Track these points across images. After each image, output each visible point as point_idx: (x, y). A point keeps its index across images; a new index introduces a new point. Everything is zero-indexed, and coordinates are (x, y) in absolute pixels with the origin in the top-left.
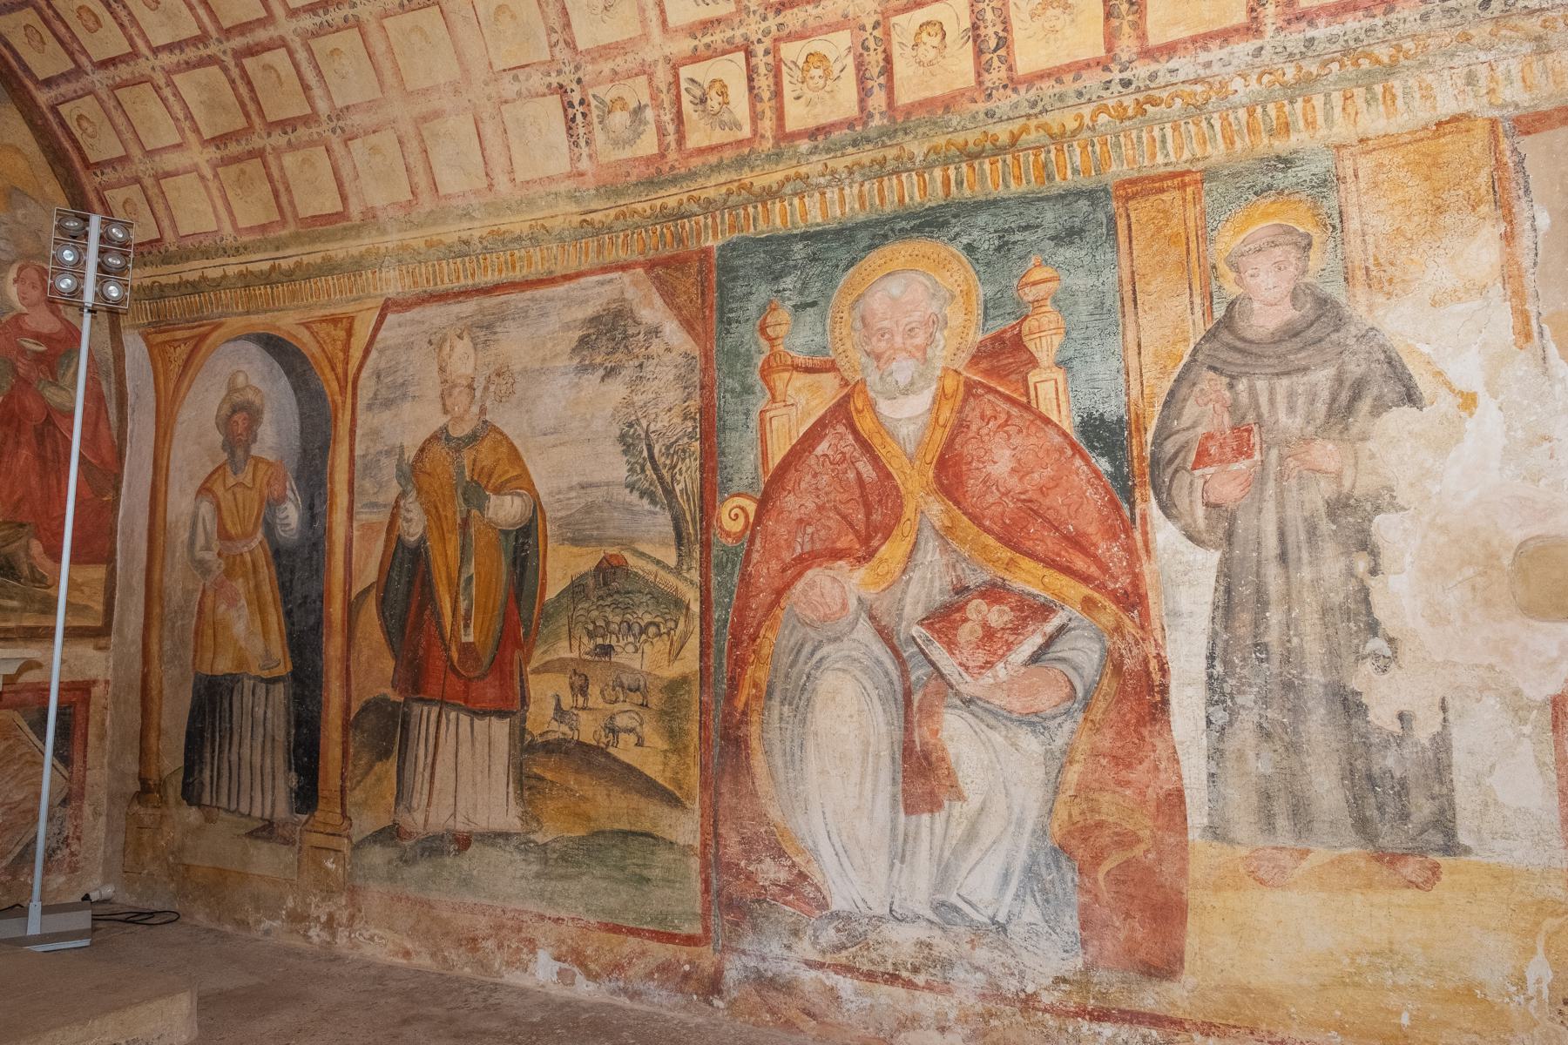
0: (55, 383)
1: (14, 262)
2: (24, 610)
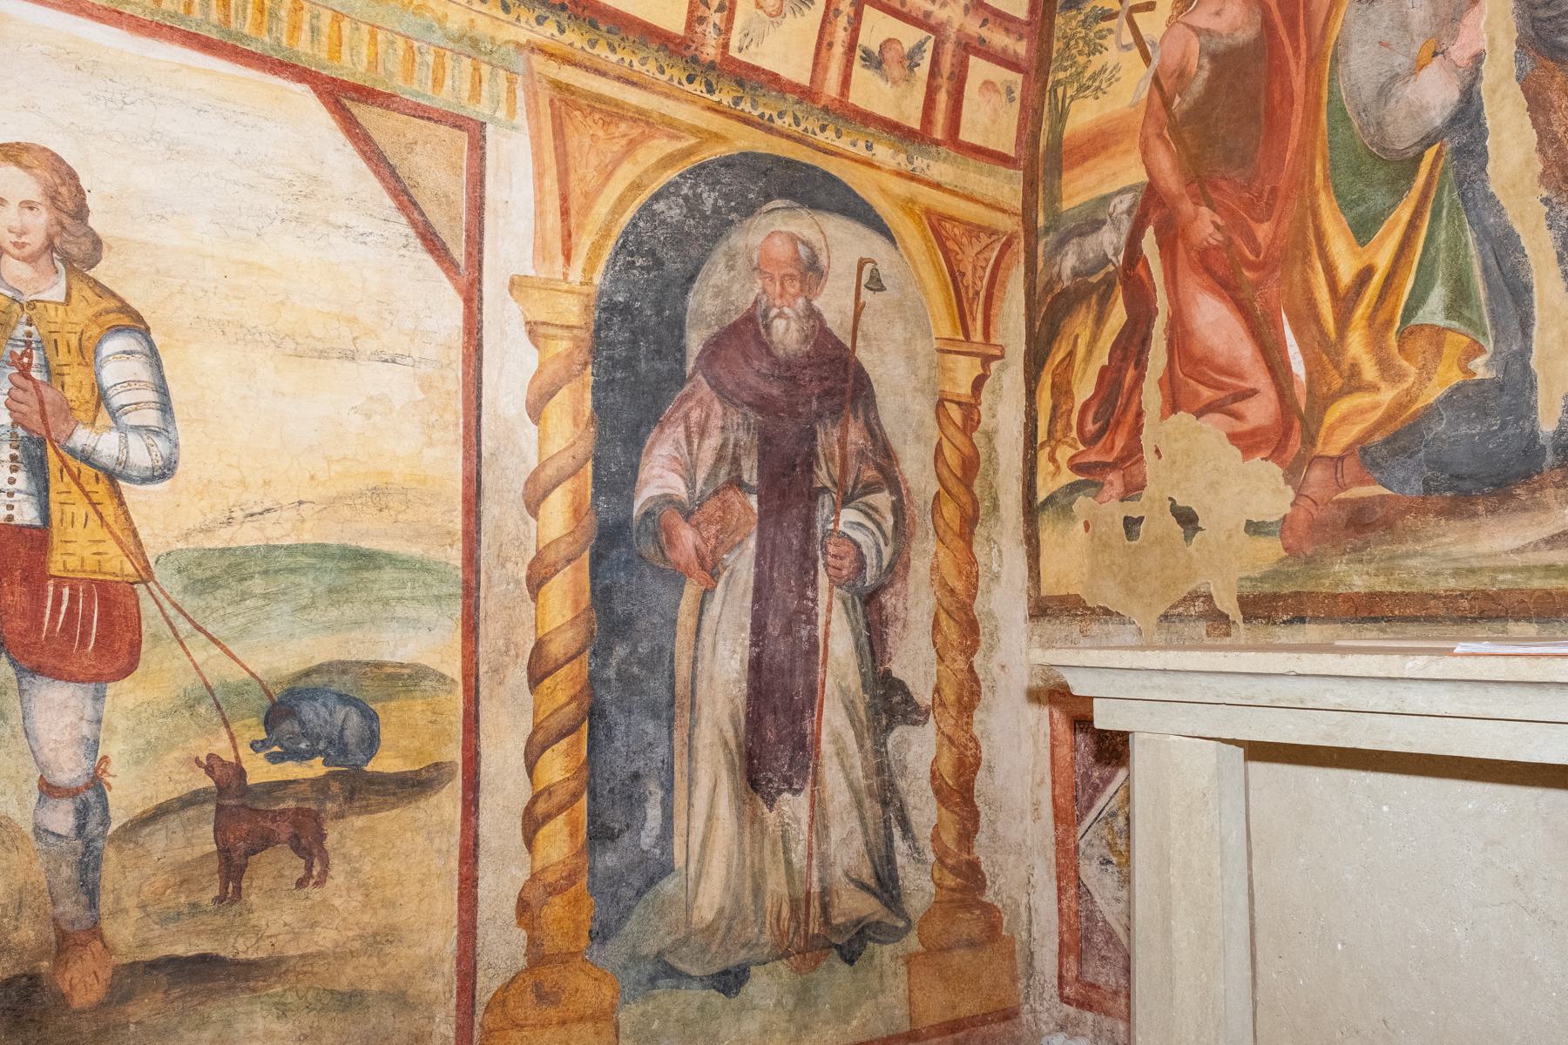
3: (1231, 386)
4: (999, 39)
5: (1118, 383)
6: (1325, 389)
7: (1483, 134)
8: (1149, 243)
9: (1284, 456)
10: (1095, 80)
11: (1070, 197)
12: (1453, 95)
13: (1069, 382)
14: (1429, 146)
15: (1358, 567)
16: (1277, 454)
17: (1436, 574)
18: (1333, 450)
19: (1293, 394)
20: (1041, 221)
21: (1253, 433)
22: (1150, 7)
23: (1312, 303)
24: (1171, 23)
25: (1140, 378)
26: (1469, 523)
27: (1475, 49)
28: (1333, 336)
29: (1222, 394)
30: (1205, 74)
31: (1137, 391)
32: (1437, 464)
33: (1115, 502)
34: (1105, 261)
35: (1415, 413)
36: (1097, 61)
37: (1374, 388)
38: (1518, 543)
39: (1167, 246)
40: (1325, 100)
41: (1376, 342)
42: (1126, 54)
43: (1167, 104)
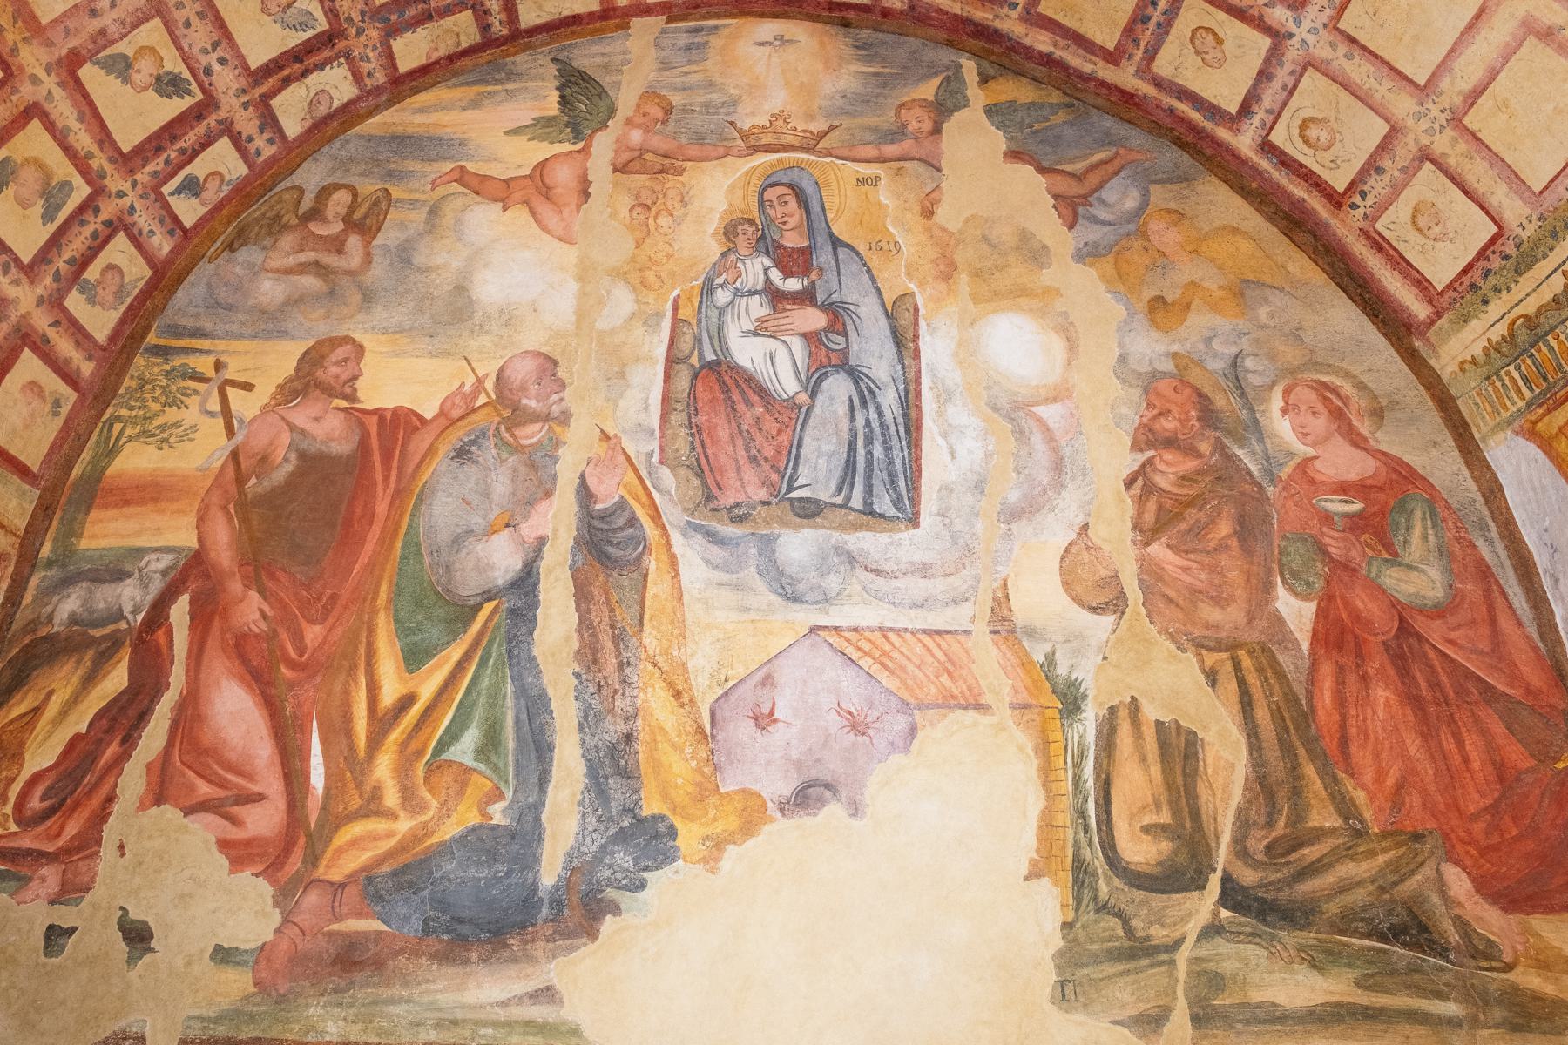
0: (1394, 559)
1: (1274, 383)
2: (1474, 1023)
3: (236, 785)
4: (65, 347)
5: (92, 757)
6: (341, 808)
7: (535, 605)
8: (180, 612)
9: (279, 875)
10: (164, 431)
11: (95, 536)
12: (518, 564)
13: (22, 744)
14: (489, 600)
15: (337, 1010)
16: (271, 870)
17: (418, 1025)
18: (336, 876)
19: (304, 807)
20: (46, 551)
21: (248, 843)
22: (248, 387)
23: (347, 718)
24: (265, 410)
25: (124, 757)
26: (459, 970)
27: (541, 532)
28: (362, 754)
29: (222, 793)
30: (289, 467)
31: (116, 771)
32: (441, 904)
33: (41, 905)
34: (119, 615)
35: (428, 848)
36: (171, 415)
37: (392, 815)
38: (504, 996)
39: (201, 619)
40: (403, 530)
41: (403, 770)
42: (208, 420)
43: (240, 480)
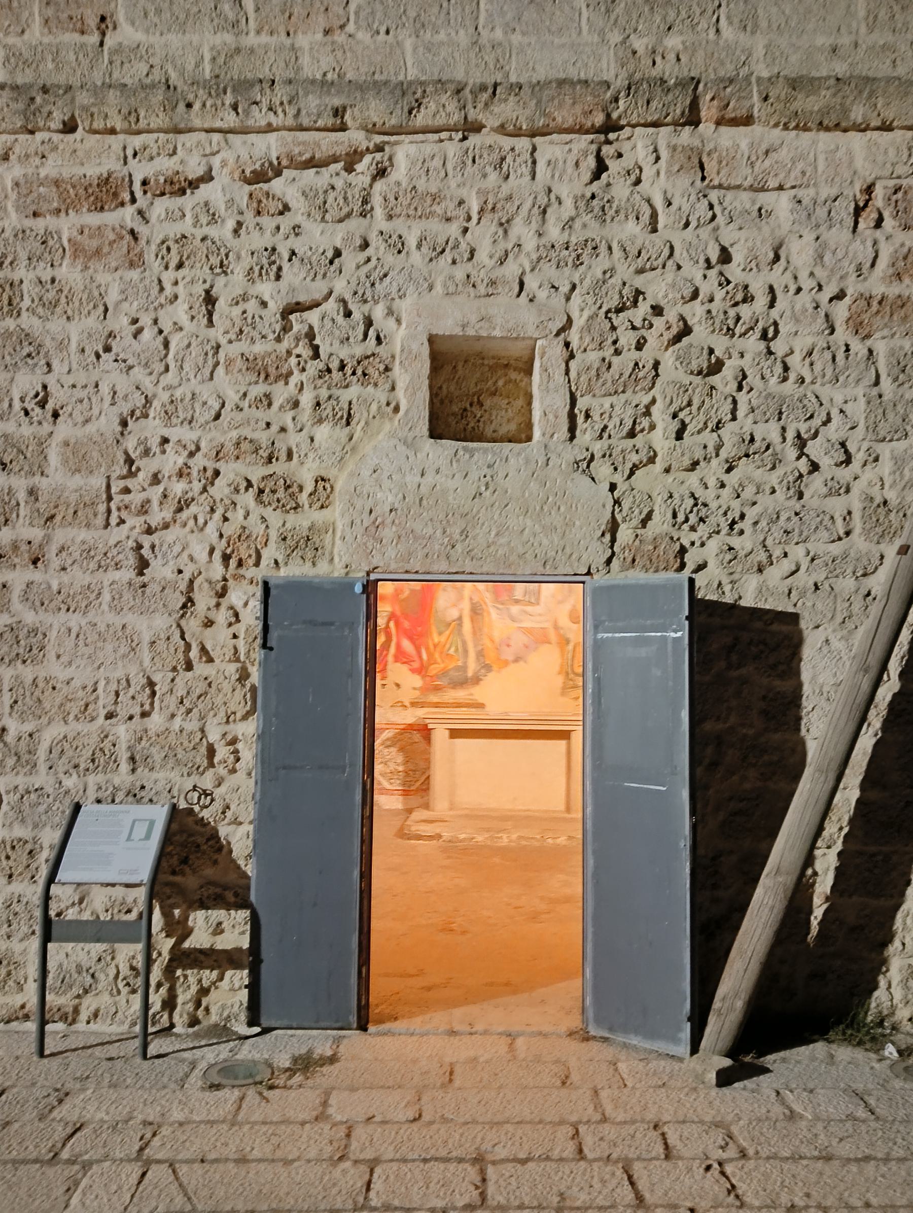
8: (392, 624)
39: (397, 624)
